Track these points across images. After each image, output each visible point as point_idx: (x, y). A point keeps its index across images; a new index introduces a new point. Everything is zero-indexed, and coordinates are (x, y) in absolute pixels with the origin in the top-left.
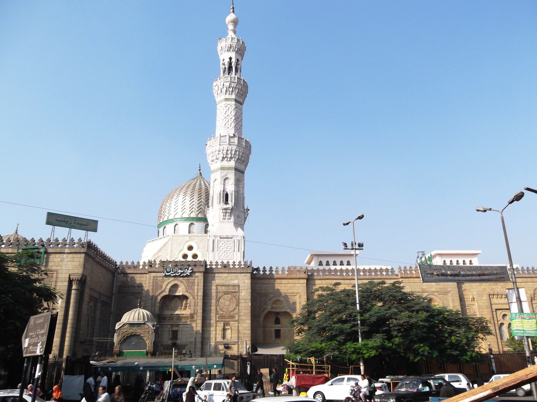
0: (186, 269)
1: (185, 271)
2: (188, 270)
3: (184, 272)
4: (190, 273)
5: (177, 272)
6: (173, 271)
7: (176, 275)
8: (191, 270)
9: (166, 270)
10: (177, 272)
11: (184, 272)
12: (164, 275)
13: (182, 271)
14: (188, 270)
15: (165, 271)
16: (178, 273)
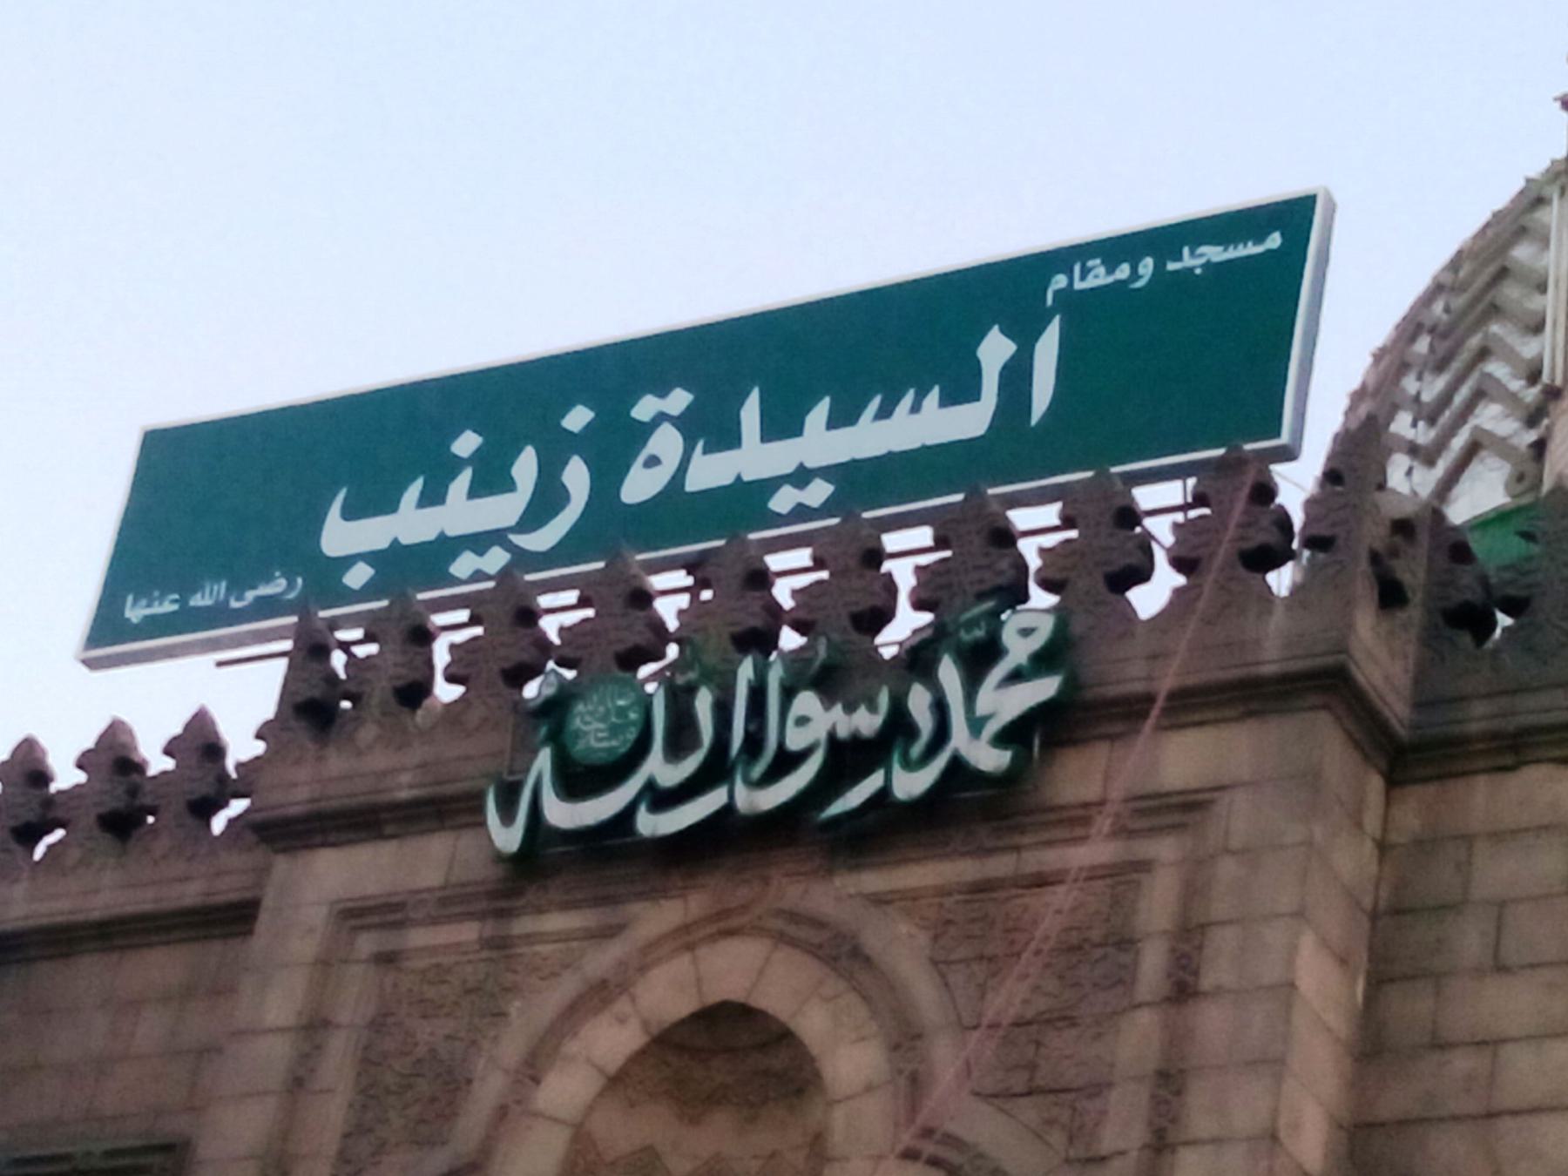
0: (949, 673)
1: (919, 702)
2: (972, 682)
3: (899, 725)
4: (1014, 734)
5: (754, 743)
6: (678, 745)
7: (728, 809)
8: (1043, 662)
9: (558, 739)
10: (754, 743)
11: (899, 725)
12: (508, 838)
13: (867, 722)
14: (972, 682)
15: (544, 761)
16: (787, 762)
